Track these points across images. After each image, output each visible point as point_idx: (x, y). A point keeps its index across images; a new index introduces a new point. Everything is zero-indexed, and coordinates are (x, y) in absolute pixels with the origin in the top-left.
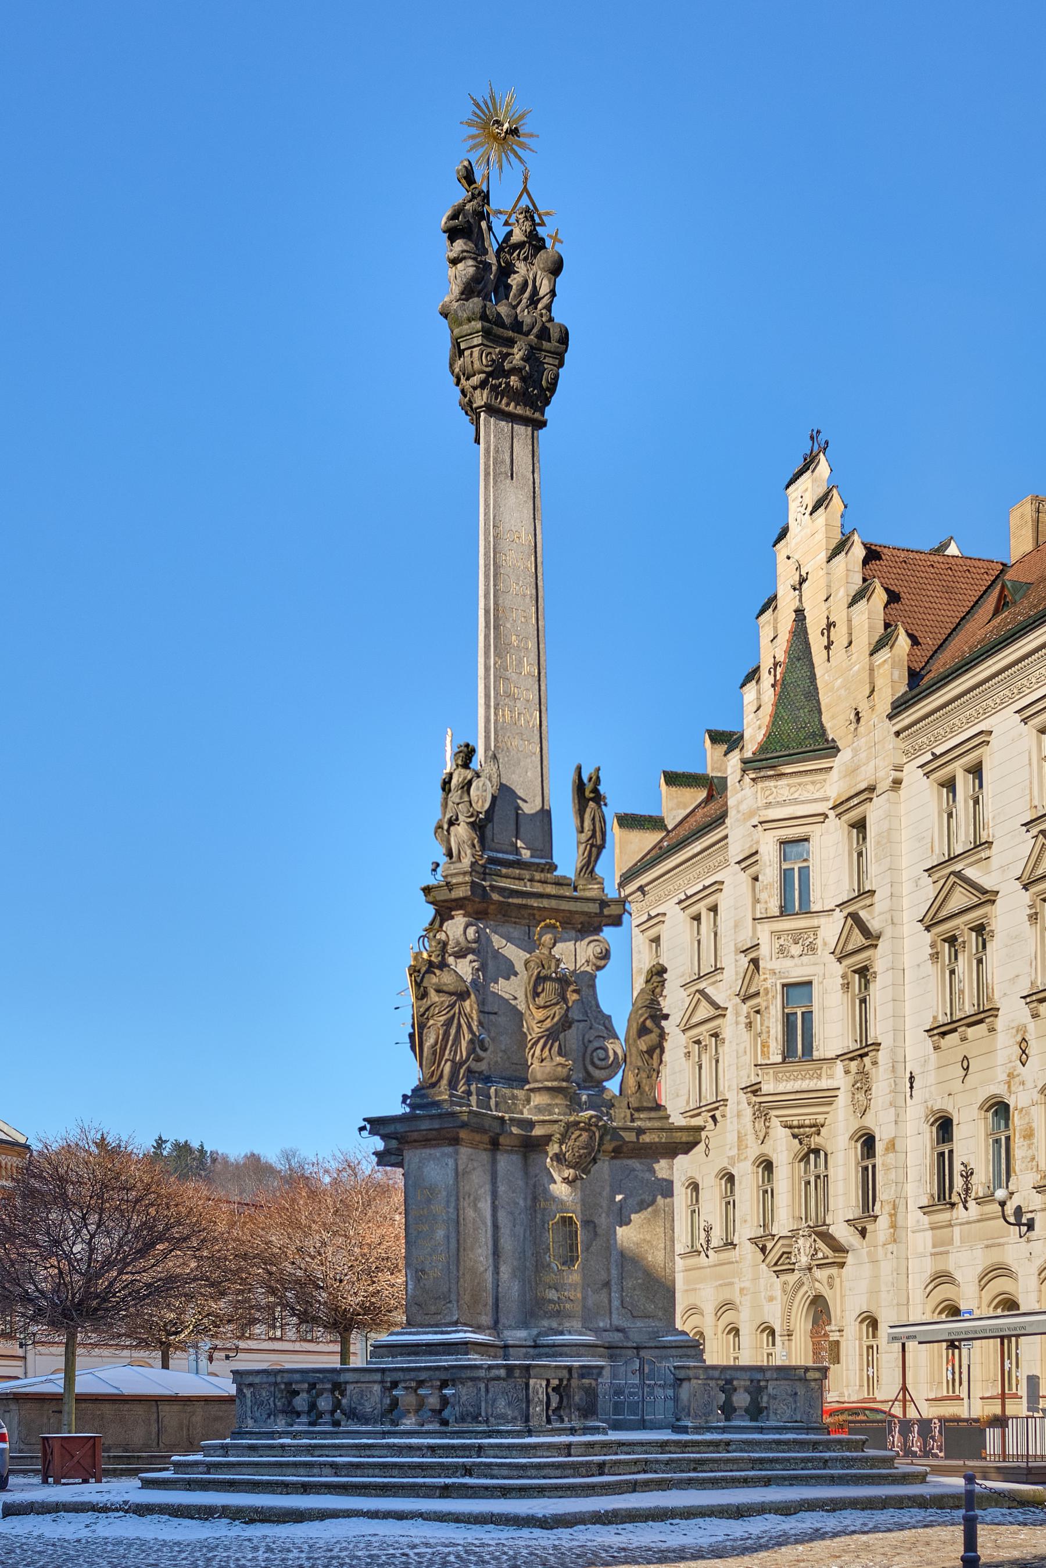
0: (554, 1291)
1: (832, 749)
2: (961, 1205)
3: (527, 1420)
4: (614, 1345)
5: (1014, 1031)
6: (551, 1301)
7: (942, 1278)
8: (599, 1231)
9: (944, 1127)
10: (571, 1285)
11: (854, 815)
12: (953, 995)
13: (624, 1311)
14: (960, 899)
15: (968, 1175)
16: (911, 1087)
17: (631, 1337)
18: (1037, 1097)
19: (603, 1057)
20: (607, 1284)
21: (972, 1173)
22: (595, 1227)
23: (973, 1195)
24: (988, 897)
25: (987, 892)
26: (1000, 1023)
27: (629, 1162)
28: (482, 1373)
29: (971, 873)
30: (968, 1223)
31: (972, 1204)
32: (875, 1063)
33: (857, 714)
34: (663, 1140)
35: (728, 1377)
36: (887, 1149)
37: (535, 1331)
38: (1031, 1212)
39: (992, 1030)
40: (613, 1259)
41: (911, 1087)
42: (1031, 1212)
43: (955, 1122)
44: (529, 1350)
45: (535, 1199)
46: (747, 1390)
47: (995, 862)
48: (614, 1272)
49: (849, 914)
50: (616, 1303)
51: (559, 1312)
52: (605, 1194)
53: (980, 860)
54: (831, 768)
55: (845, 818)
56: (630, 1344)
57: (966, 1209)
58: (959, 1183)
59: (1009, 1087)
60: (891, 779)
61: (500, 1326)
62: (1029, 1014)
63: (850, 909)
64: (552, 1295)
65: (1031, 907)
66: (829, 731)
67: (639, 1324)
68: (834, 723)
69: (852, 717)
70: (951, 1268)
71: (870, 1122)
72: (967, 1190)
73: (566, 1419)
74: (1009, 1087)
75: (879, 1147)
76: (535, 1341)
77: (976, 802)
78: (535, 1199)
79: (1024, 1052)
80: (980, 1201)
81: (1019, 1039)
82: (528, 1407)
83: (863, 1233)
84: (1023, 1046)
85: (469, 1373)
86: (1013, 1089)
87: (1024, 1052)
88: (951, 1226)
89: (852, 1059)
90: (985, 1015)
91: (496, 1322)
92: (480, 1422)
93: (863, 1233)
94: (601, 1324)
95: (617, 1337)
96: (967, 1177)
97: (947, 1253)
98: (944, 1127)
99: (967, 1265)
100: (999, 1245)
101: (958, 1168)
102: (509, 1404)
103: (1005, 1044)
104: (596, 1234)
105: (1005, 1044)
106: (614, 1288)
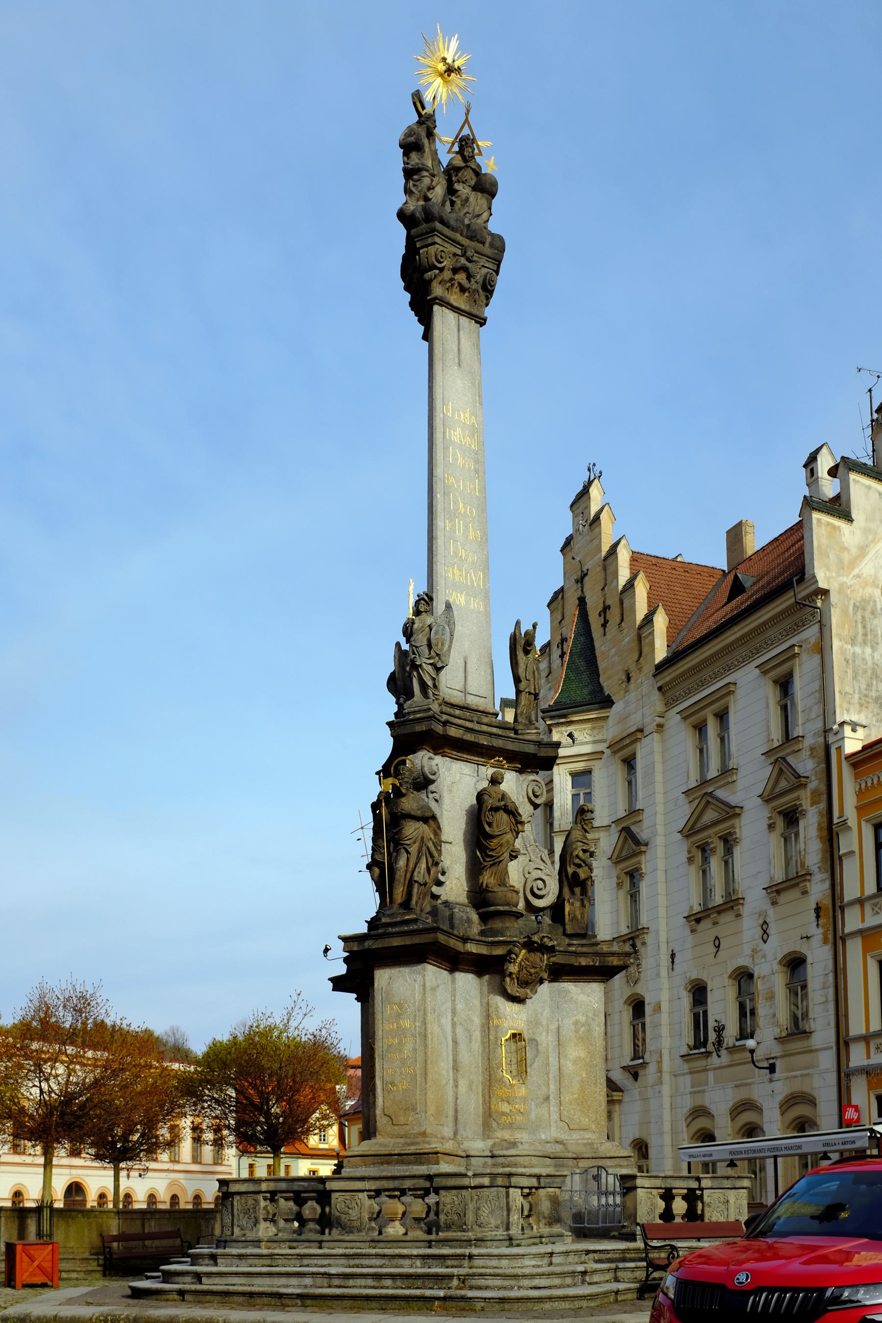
0: (506, 1104)
1: (607, 702)
2: (715, 1054)
3: (508, 1229)
4: (557, 1155)
5: (757, 916)
6: (503, 1114)
7: (699, 1112)
8: (540, 1048)
9: (699, 993)
10: (521, 1098)
11: (626, 752)
12: (706, 891)
13: (562, 1124)
14: (710, 815)
15: (720, 1030)
16: (673, 962)
17: (570, 1149)
18: (776, 967)
19: (540, 887)
20: (547, 1098)
21: (723, 1028)
22: (537, 1045)
23: (725, 1046)
24: (732, 812)
25: (800, 777)
26: (746, 910)
27: (565, 984)
28: (465, 1182)
29: (721, 794)
30: (720, 1068)
31: (723, 1052)
32: (644, 944)
33: (628, 674)
34: (597, 964)
35: (668, 1186)
36: (655, 1010)
37: (490, 1142)
38: (773, 1058)
39: (739, 915)
40: (551, 1076)
41: (673, 962)
42: (773, 1058)
43: (709, 989)
44: (487, 1159)
45: (488, 1017)
46: (685, 1198)
47: (740, 785)
48: (553, 1087)
49: (623, 829)
50: (555, 1117)
51: (511, 1124)
52: (545, 1013)
53: (728, 783)
54: (608, 717)
55: (618, 755)
56: (570, 1155)
57: (719, 1056)
58: (712, 1036)
59: (753, 959)
60: (655, 723)
61: (459, 1137)
62: (769, 902)
63: (624, 825)
64: (505, 1107)
65: (770, 818)
66: (605, 689)
67: (576, 1136)
68: (609, 683)
69: (624, 677)
70: (707, 1103)
71: (640, 989)
72: (719, 1042)
73: (535, 1227)
74: (753, 959)
75: (648, 1009)
76: (491, 1151)
77: (722, 739)
78: (488, 1017)
79: (765, 932)
80: (732, 1050)
81: (761, 922)
82: (508, 1215)
83: (635, 1076)
84: (765, 927)
85: (451, 1182)
86: (756, 961)
87: (765, 932)
88: (706, 1070)
89: (624, 941)
90: (732, 903)
91: (456, 1133)
92: (464, 1231)
93: (635, 1076)
94: (543, 1137)
95: (558, 1148)
96: (719, 1032)
97: (703, 1091)
98: (699, 993)
99: (720, 1101)
100: (747, 1084)
101: (711, 1024)
102: (492, 1212)
103: (749, 926)
104: (538, 1051)
105: (749, 926)
106: (553, 1101)
